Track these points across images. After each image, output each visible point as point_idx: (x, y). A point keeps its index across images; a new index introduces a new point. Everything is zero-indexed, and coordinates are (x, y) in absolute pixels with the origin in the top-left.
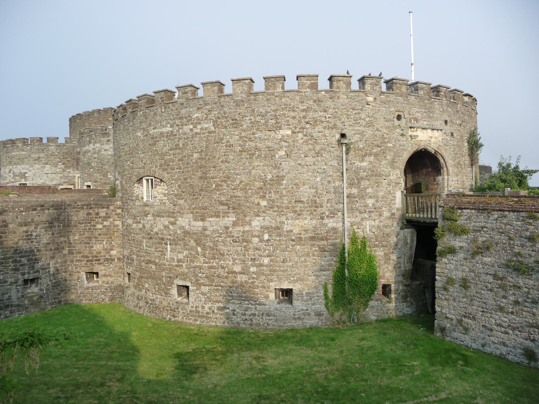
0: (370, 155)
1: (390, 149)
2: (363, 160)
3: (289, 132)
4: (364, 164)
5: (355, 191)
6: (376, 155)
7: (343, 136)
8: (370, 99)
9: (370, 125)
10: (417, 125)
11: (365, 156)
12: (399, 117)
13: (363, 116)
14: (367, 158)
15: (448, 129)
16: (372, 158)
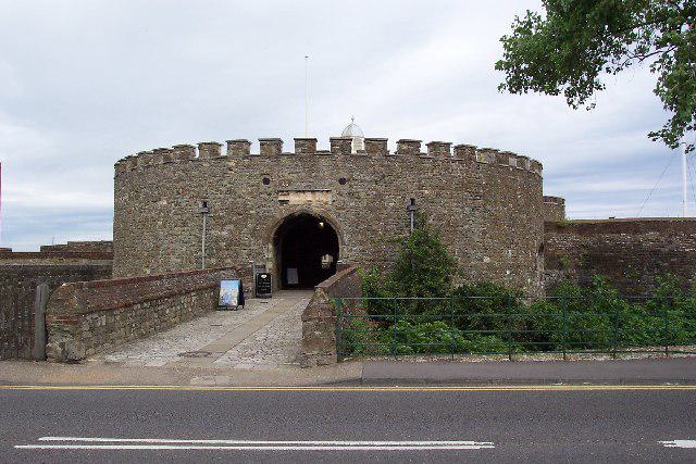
0: (230, 223)
1: (251, 216)
2: (222, 230)
3: (165, 203)
4: (224, 233)
5: (213, 261)
6: (235, 223)
7: (205, 204)
8: (232, 164)
9: (230, 191)
10: (290, 188)
11: (226, 224)
12: (266, 181)
13: (225, 183)
14: (228, 227)
15: (345, 188)
16: (232, 227)
